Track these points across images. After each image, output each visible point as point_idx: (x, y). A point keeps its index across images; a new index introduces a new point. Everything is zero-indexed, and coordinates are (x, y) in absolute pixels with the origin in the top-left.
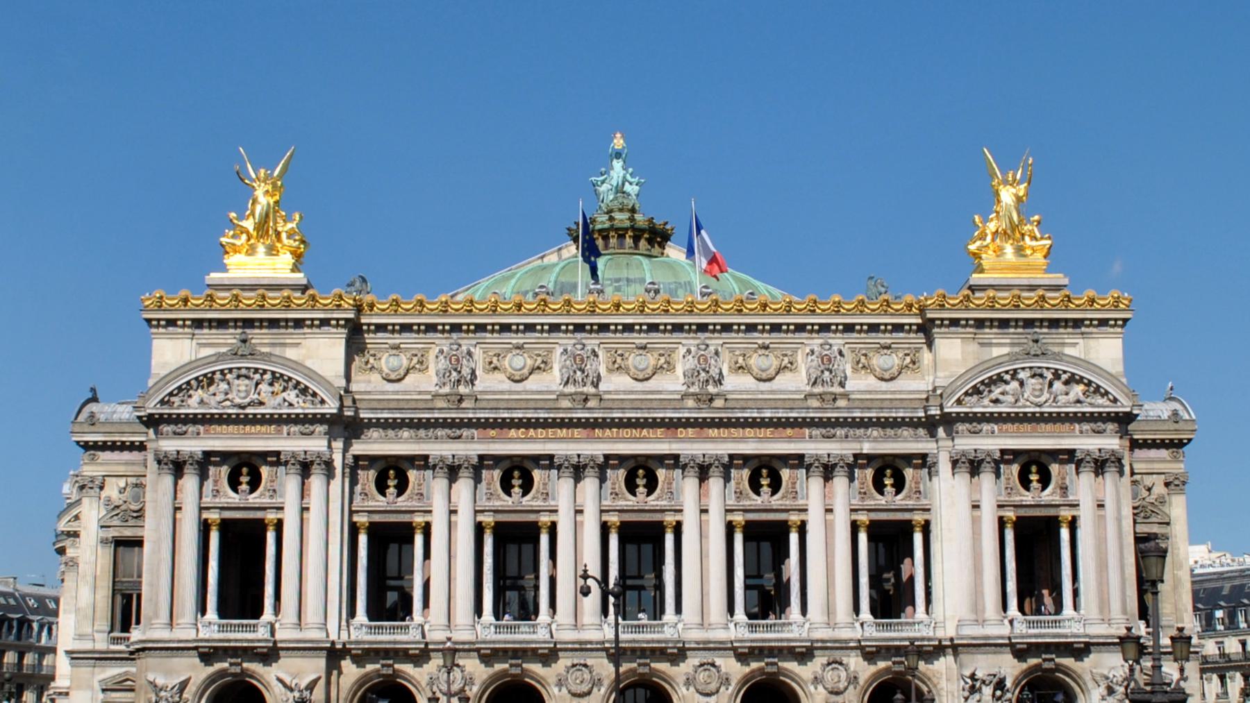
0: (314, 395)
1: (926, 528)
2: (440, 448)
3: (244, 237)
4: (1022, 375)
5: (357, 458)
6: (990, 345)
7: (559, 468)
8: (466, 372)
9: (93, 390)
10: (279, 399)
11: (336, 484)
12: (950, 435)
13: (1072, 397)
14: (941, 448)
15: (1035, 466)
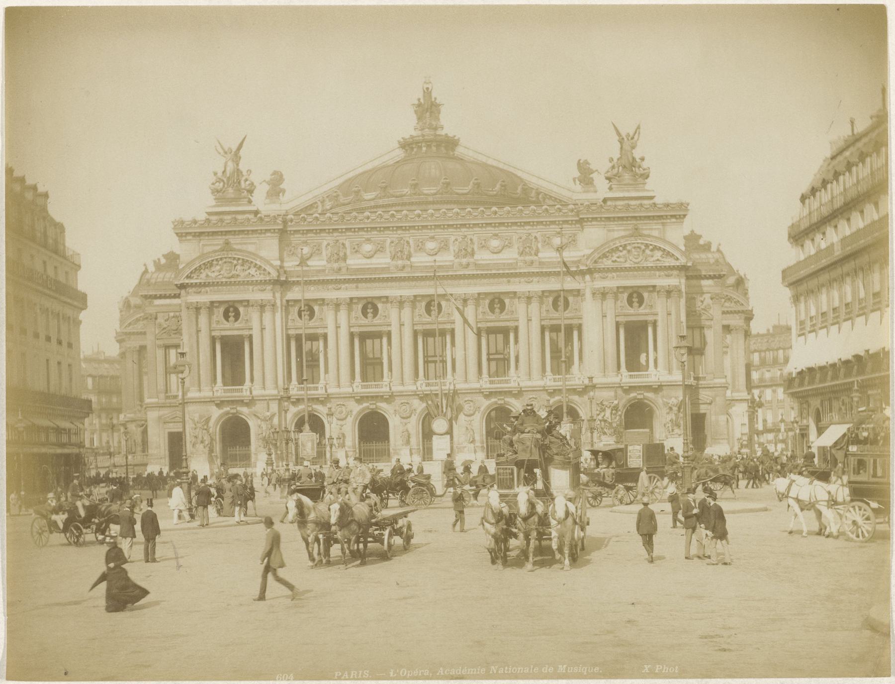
0: (265, 270)
1: (580, 328)
2: (331, 294)
3: (222, 184)
4: (629, 248)
5: (288, 301)
6: (613, 230)
7: (391, 302)
8: (341, 254)
9: (145, 265)
10: (247, 272)
11: (278, 315)
12: (593, 279)
13: (655, 258)
14: (587, 285)
15: (636, 296)
